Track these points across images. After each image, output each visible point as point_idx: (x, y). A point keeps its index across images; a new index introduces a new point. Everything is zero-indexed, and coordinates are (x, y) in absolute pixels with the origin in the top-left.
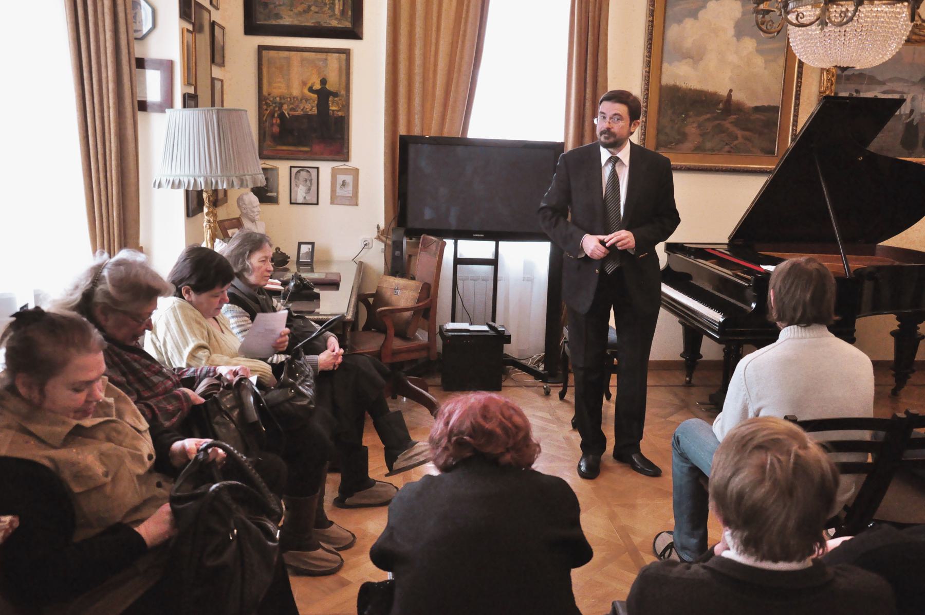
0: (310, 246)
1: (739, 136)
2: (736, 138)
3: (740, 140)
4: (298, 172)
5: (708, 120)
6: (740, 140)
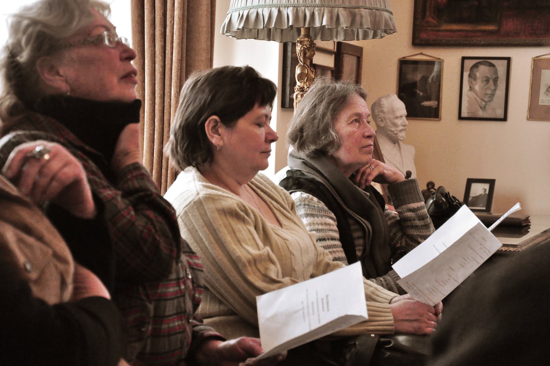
0: (487, 186)
4: (476, 66)
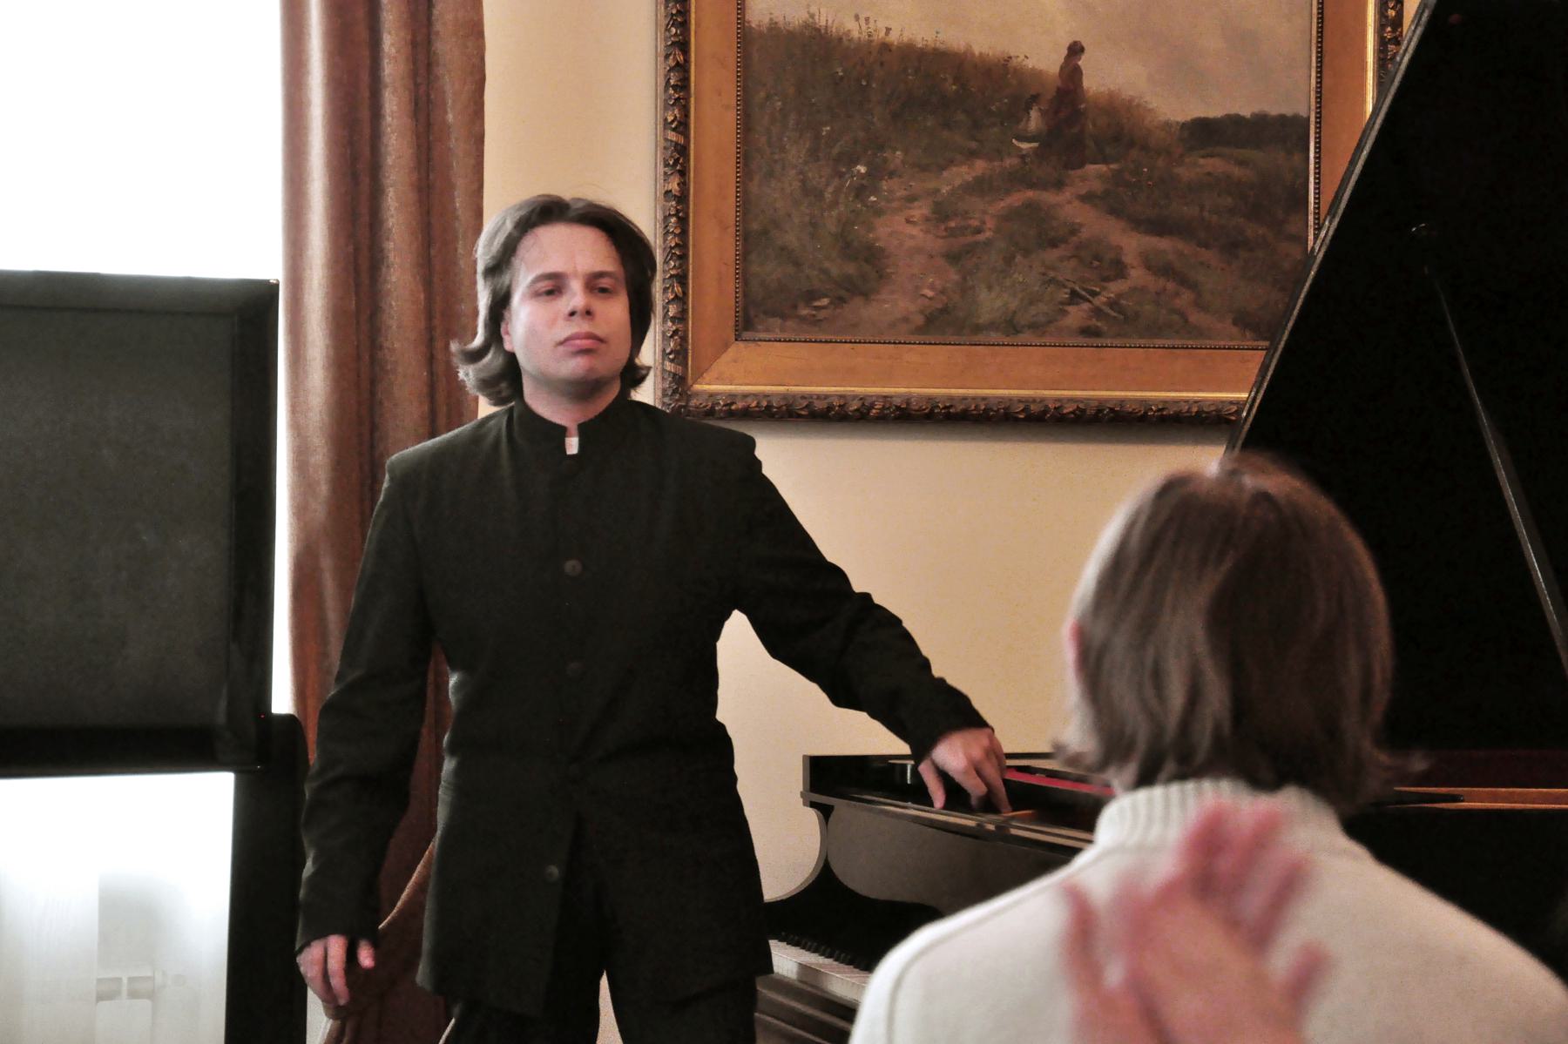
1: (1129, 258)
2: (1118, 269)
3: (1134, 273)
5: (980, 187)
6: (1137, 275)
